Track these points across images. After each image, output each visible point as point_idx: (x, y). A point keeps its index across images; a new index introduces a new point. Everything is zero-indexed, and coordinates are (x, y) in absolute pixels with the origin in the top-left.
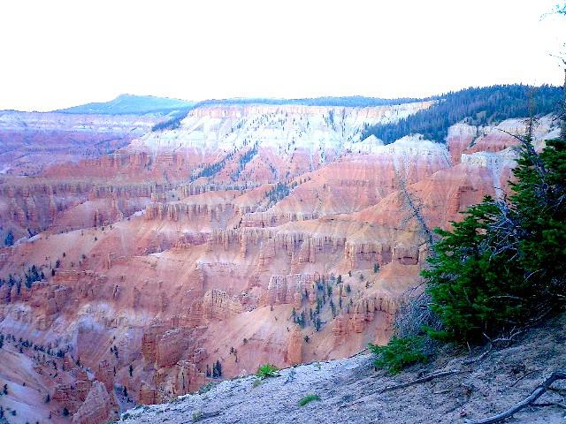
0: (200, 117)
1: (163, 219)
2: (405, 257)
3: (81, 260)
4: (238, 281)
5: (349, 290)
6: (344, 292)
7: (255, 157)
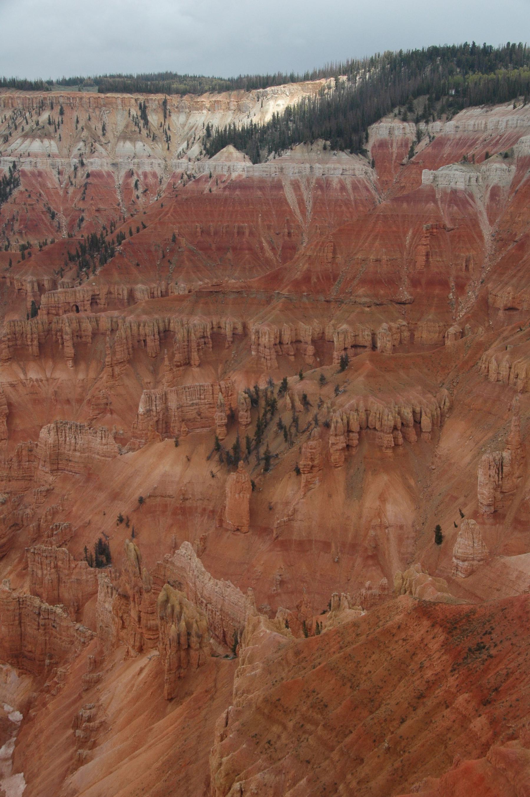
2: (354, 346)
4: (66, 407)
5: (304, 399)
6: (298, 404)
7: (15, 192)
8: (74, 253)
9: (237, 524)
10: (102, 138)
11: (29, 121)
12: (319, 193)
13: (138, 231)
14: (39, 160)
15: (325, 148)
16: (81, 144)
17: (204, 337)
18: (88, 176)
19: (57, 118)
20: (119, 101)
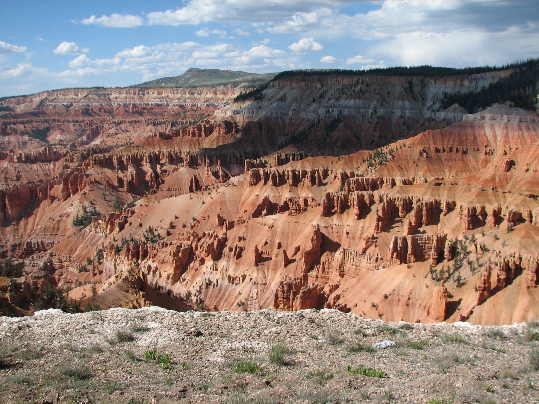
0: (281, 89)
1: (265, 184)
3: (192, 221)
8: (365, 158)
9: (437, 316)
10: (387, 100)
11: (350, 90)
12: (505, 131)
13: (401, 148)
14: (352, 110)
15: (510, 106)
16: (375, 102)
17: (431, 209)
18: (378, 118)
19: (364, 88)
20: (397, 80)
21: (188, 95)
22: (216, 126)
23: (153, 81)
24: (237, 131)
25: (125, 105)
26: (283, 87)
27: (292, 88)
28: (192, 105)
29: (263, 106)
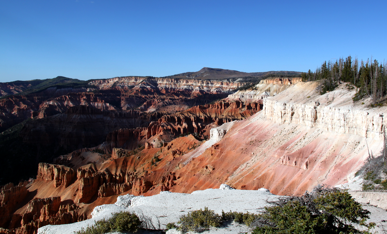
21: (205, 85)
22: (231, 103)
23: (180, 74)
24: (243, 106)
25: (166, 89)
26: (269, 84)
27: (274, 84)
28: (207, 91)
29: (257, 93)
